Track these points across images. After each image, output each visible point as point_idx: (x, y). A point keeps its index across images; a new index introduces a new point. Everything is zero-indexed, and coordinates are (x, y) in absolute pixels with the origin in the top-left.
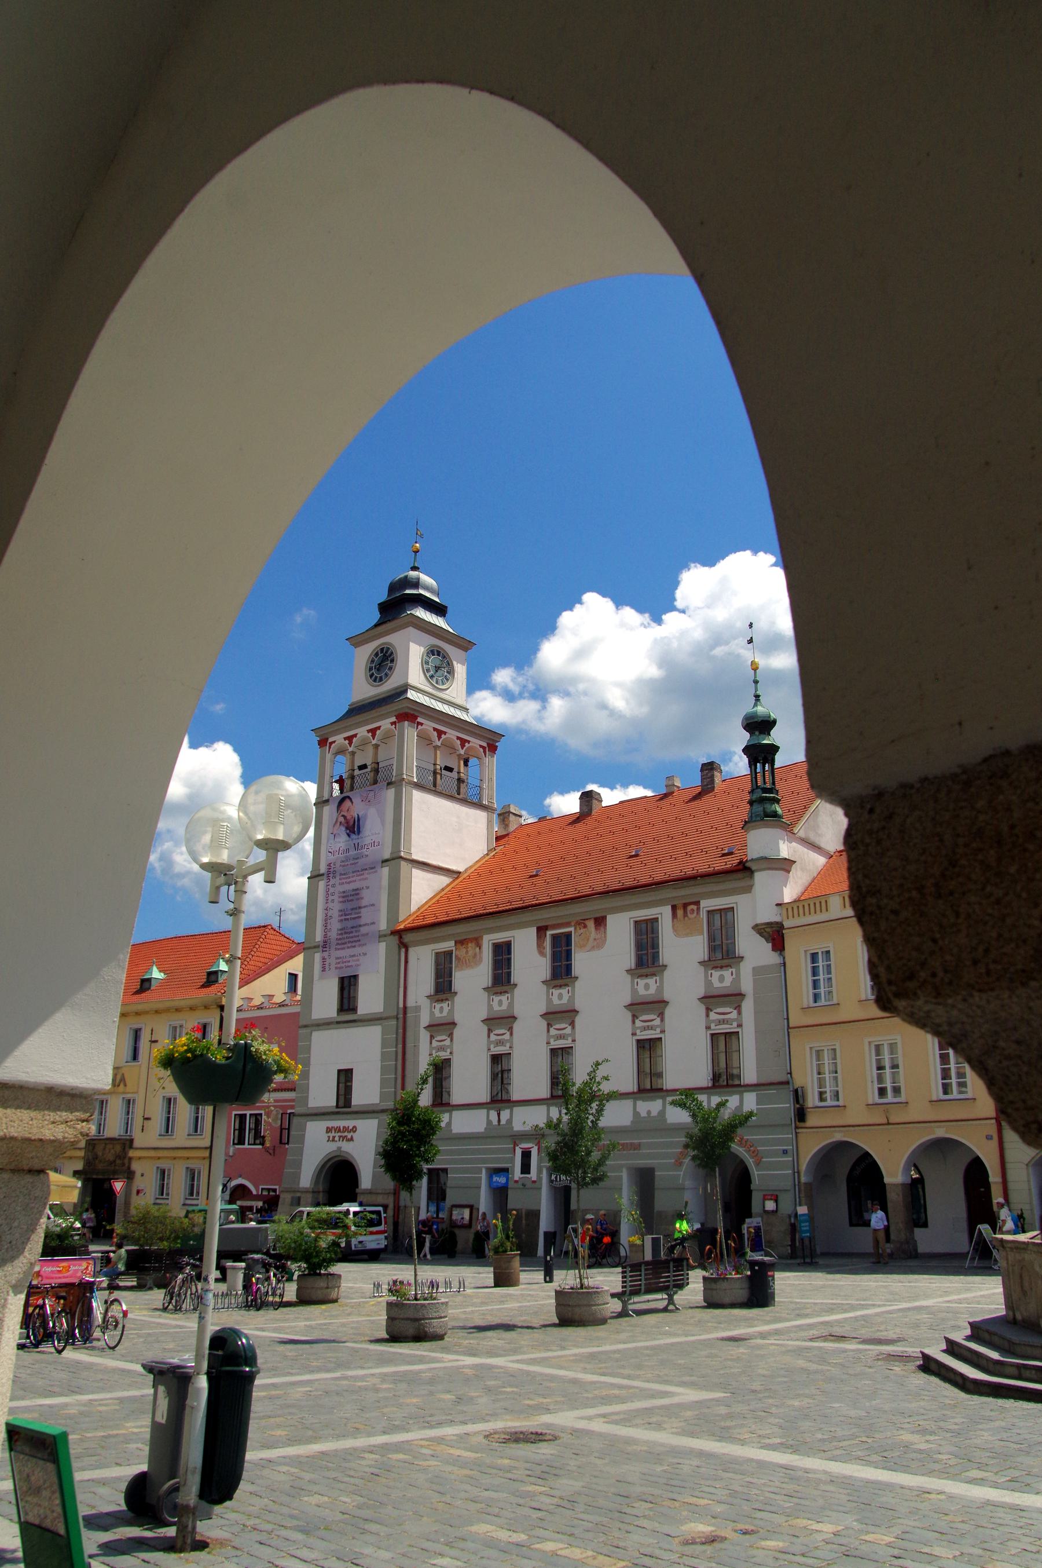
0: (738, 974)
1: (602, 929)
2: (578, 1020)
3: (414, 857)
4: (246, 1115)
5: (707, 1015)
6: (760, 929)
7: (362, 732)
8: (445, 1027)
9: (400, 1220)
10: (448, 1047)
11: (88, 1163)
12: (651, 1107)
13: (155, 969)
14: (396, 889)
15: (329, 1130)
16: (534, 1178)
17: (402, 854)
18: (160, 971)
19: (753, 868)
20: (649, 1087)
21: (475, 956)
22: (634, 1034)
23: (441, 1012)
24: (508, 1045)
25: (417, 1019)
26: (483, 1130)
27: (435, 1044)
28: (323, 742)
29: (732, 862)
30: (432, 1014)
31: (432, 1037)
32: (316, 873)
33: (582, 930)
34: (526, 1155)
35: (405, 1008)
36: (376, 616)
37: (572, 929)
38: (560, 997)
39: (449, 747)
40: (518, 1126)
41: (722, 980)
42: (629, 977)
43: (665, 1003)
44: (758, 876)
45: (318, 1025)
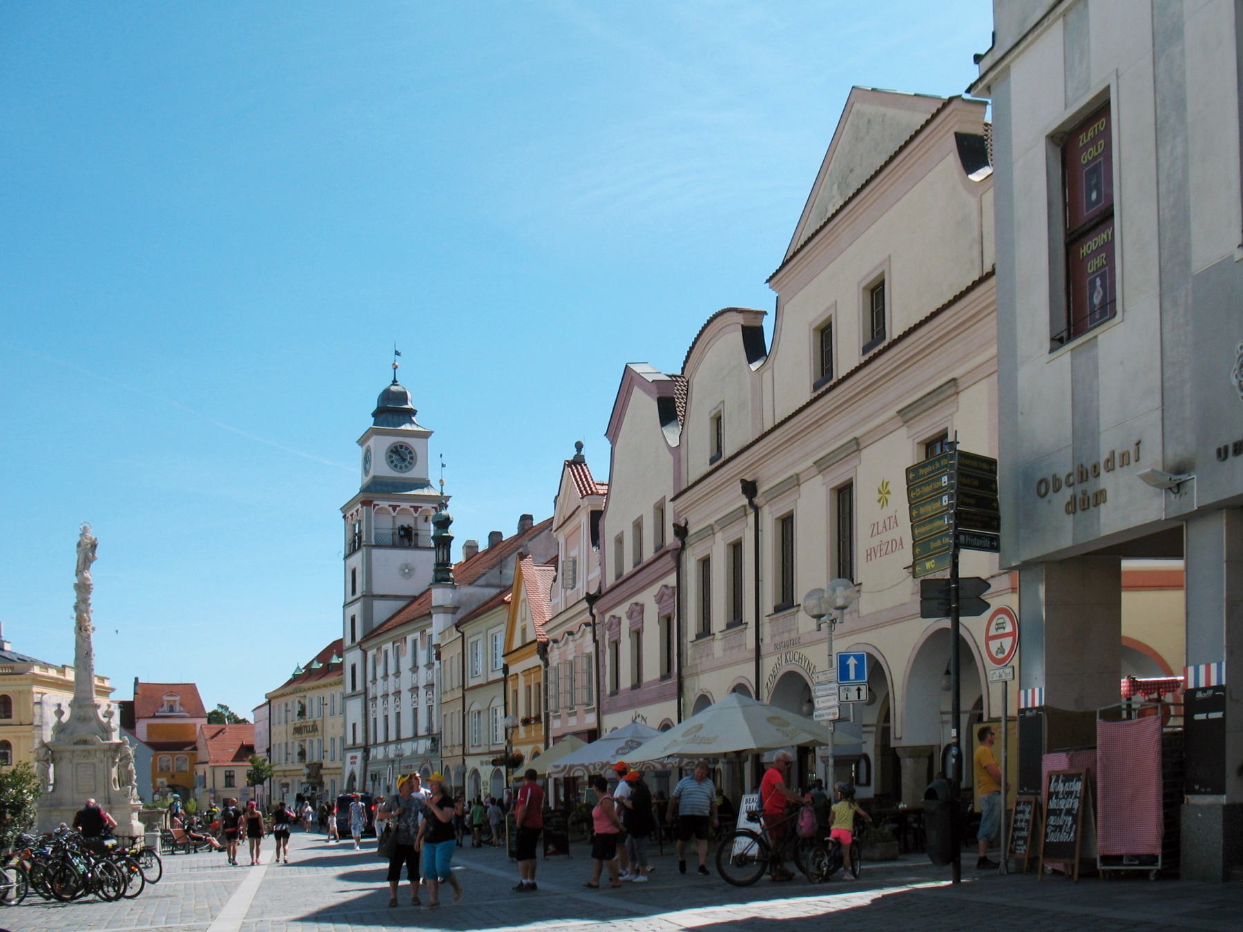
7: (354, 511)
12: (415, 745)
19: (432, 612)
28: (344, 517)
42: (410, 673)
44: (434, 616)
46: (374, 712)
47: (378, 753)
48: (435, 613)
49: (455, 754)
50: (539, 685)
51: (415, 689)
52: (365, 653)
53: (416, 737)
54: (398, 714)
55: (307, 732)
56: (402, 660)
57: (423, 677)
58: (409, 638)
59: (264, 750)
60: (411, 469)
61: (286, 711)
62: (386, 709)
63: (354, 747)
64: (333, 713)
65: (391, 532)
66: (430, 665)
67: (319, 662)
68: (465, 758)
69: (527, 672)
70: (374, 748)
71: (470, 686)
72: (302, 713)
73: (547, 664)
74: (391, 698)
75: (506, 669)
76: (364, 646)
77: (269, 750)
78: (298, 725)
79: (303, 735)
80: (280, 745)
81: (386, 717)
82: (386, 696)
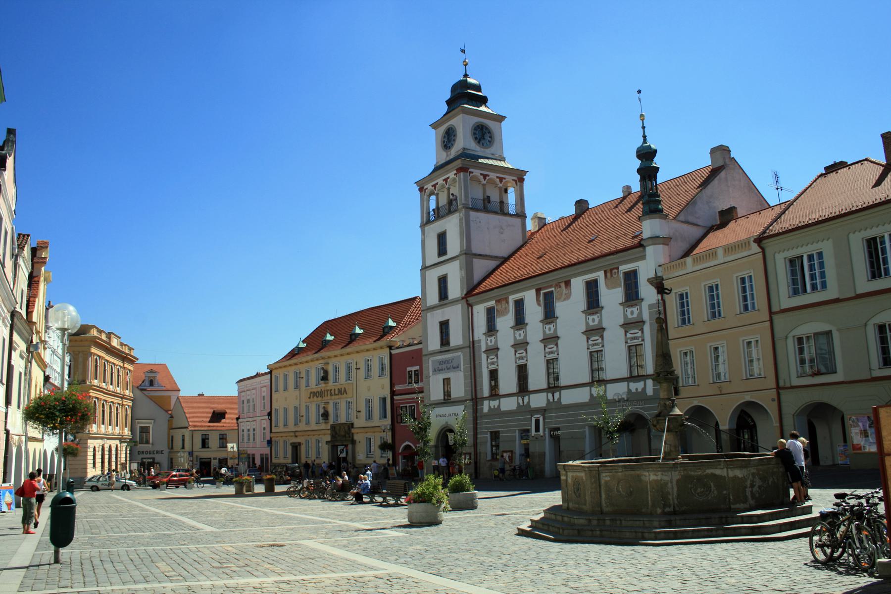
1: (569, 287)
2: (560, 342)
4: (406, 406)
7: (440, 181)
8: (493, 350)
9: (478, 460)
10: (495, 362)
11: (333, 436)
12: (597, 391)
13: (357, 328)
16: (542, 434)
19: (645, 244)
20: (637, 374)
21: (506, 308)
22: (588, 349)
23: (491, 341)
24: (525, 359)
25: (480, 347)
26: (515, 408)
27: (489, 361)
28: (421, 190)
29: (636, 241)
30: (487, 343)
31: (488, 357)
33: (559, 289)
34: (537, 421)
35: (473, 341)
37: (553, 289)
38: (550, 329)
40: (533, 405)
41: (633, 313)
43: (604, 329)
44: (647, 248)
48: (652, 244)
49: (723, 393)
55: (331, 395)
60: (490, 147)
63: (447, 400)
64: (368, 376)
65: (482, 198)
67: (331, 335)
68: (781, 391)
71: (784, 306)
72: (325, 378)
76: (471, 300)
77: (270, 414)
78: (315, 390)
79: (324, 398)
80: (286, 410)
82: (521, 345)
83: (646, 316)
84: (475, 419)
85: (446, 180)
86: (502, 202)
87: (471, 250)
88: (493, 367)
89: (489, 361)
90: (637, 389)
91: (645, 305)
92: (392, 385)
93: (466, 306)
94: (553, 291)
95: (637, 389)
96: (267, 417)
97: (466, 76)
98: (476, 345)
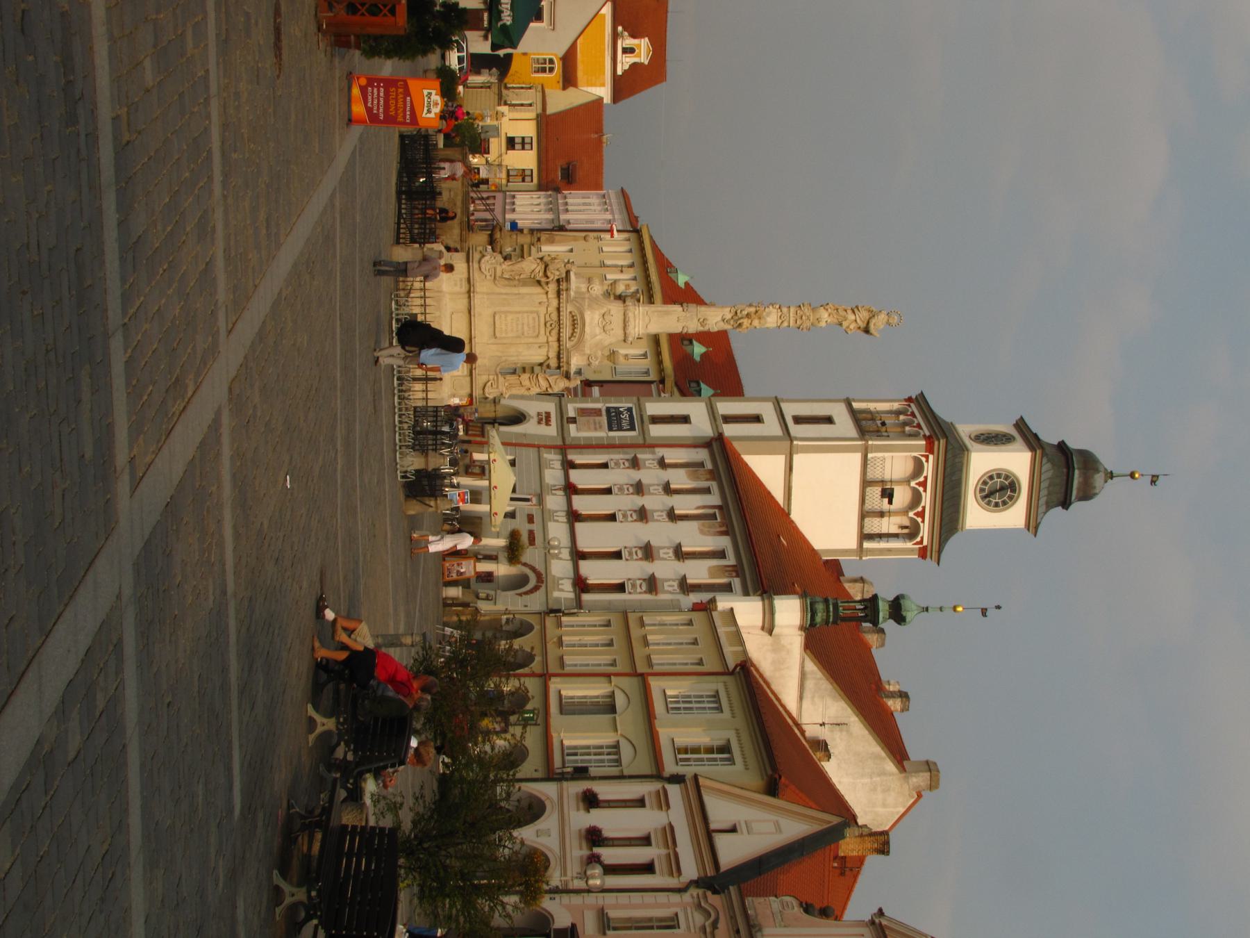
0: (673, 593)
2: (639, 524)
3: (798, 459)
5: (639, 579)
6: (713, 601)
7: (920, 419)
8: (635, 464)
12: (565, 554)
14: (764, 444)
15: (548, 415)
17: (795, 442)
18: (703, 356)
19: (764, 595)
22: (625, 548)
28: (910, 400)
30: (649, 460)
31: (627, 460)
32: (779, 400)
36: (1050, 437)
37: (719, 520)
39: (916, 499)
44: (759, 598)
45: (639, 405)
46: (617, 464)
47: (554, 475)
50: (648, 868)
51: (648, 552)
52: (707, 444)
53: (578, 555)
54: (612, 518)
56: (694, 525)
57: (666, 569)
58: (724, 542)
59: (561, 224)
61: (622, 266)
62: (621, 489)
65: (887, 477)
66: (686, 587)
68: (543, 677)
69: (669, 833)
70: (563, 464)
73: (679, 891)
74: (639, 501)
75: (677, 779)
81: (608, 491)
82: (639, 488)
83: (662, 597)
84: (539, 447)
85: (919, 426)
86: (881, 514)
87: (797, 453)
88: (612, 464)
89: (621, 462)
90: (562, 584)
91: (681, 597)
92: (600, 383)
93: (709, 440)
94: (716, 519)
95: (562, 584)
96: (557, 224)
97: (1111, 475)
98: (647, 449)
